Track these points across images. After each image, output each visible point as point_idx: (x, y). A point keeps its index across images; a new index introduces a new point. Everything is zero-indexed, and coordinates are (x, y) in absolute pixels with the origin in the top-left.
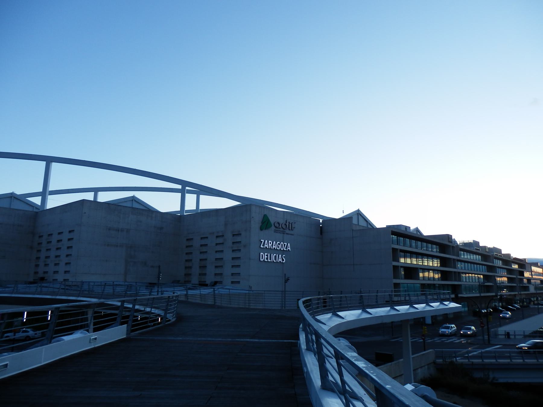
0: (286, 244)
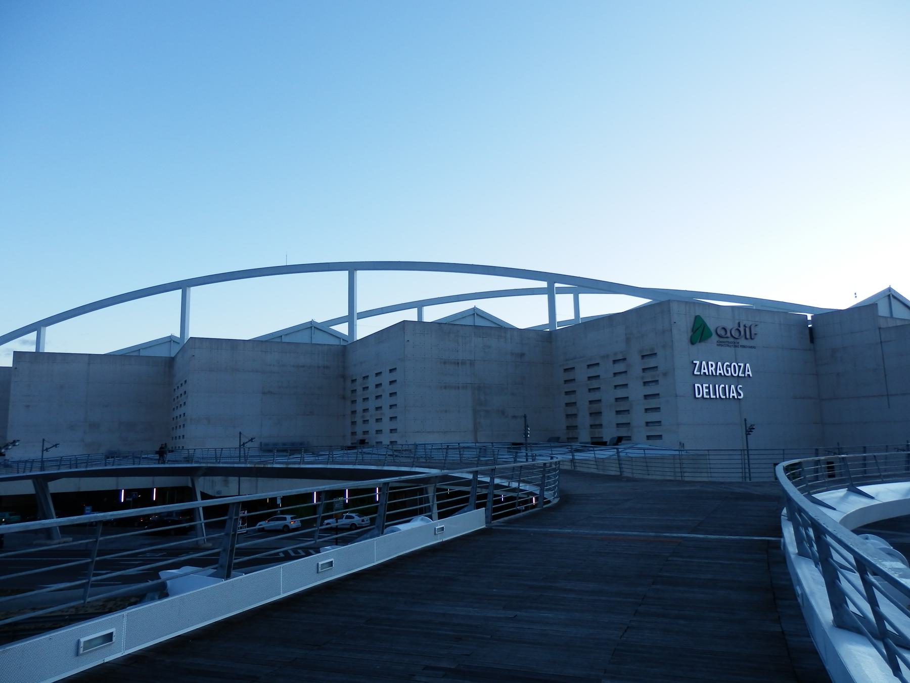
0: (742, 365)
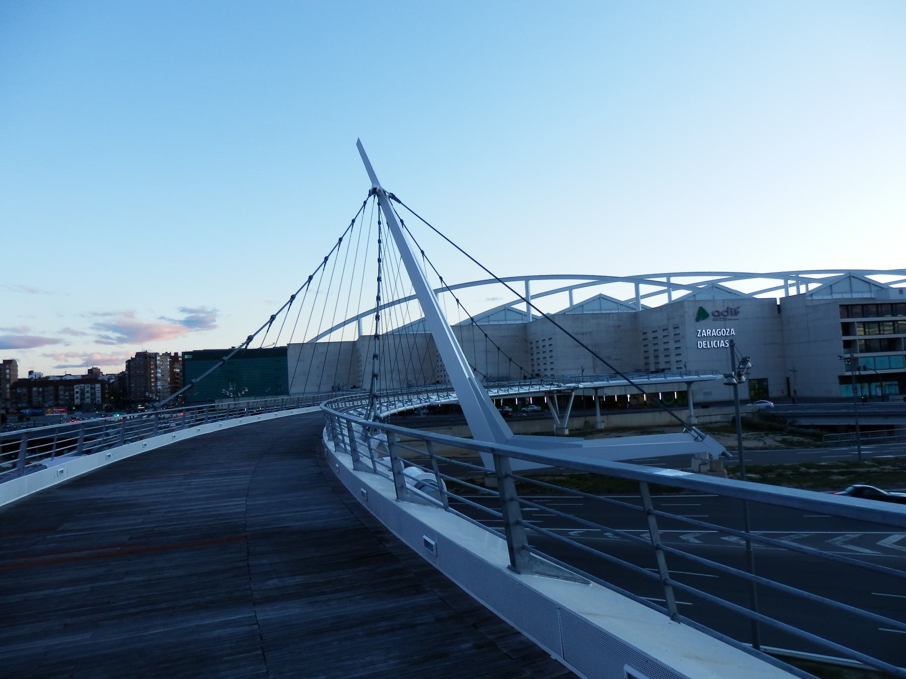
0: (729, 330)
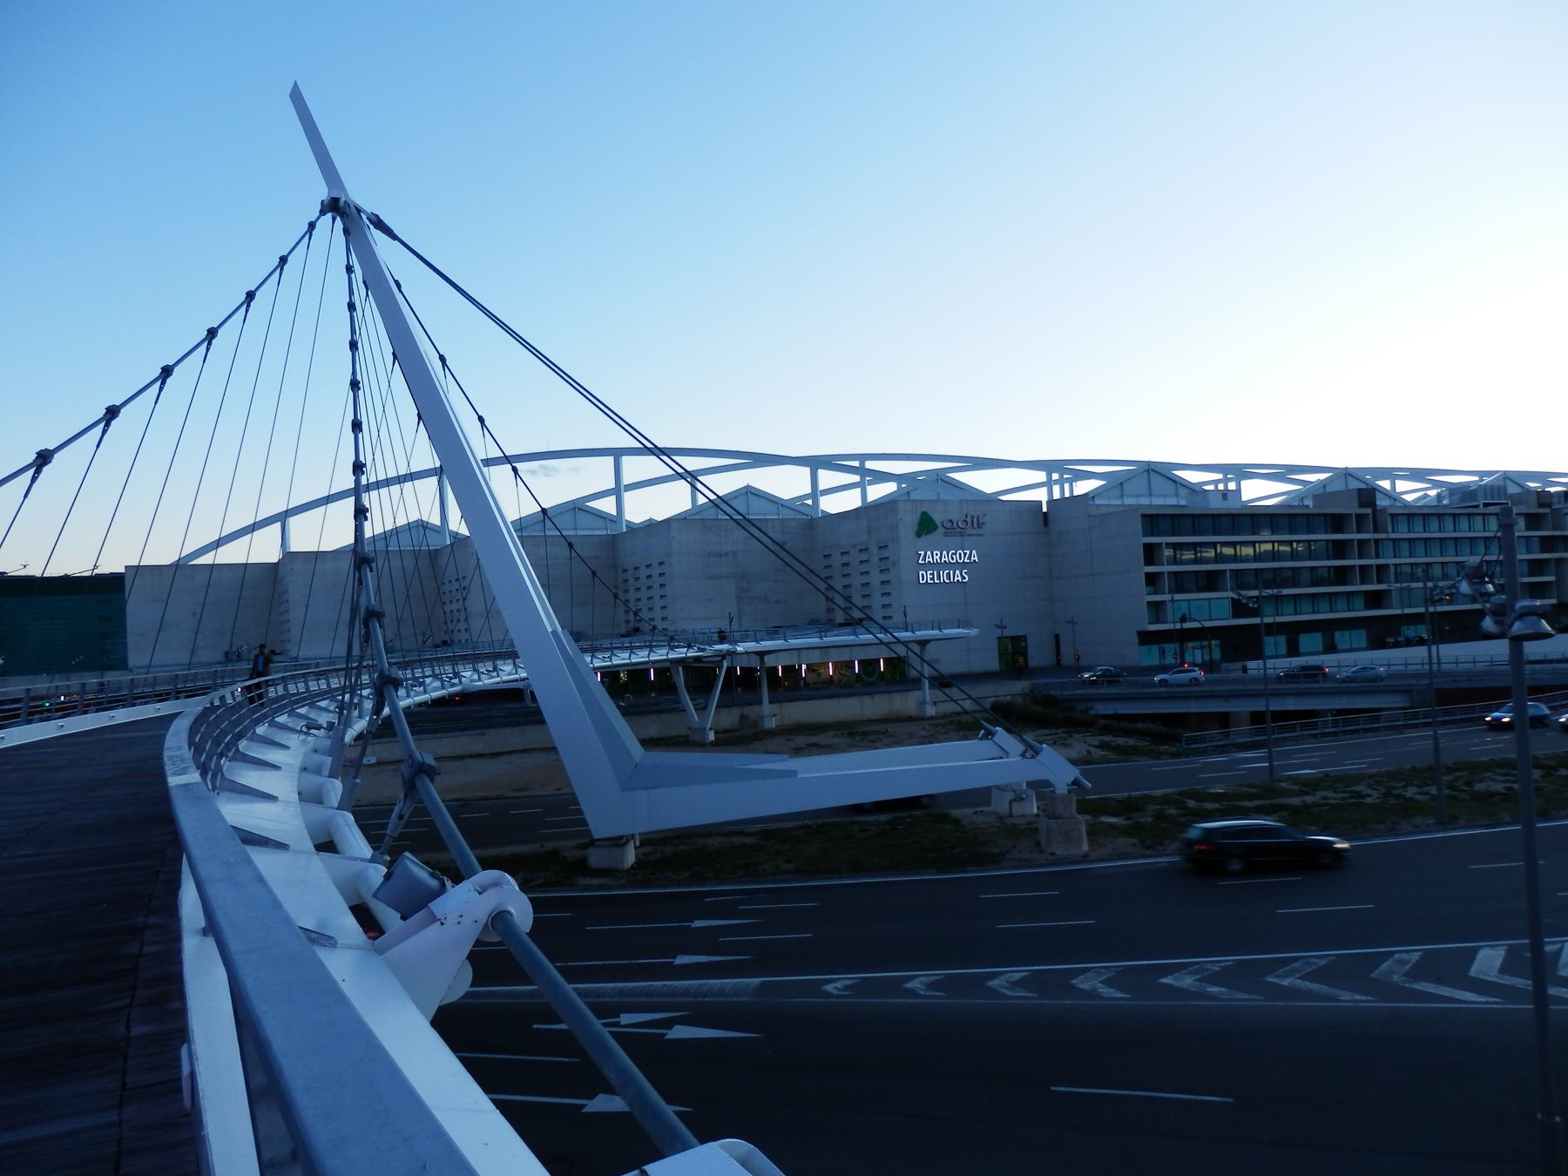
0: (968, 552)
